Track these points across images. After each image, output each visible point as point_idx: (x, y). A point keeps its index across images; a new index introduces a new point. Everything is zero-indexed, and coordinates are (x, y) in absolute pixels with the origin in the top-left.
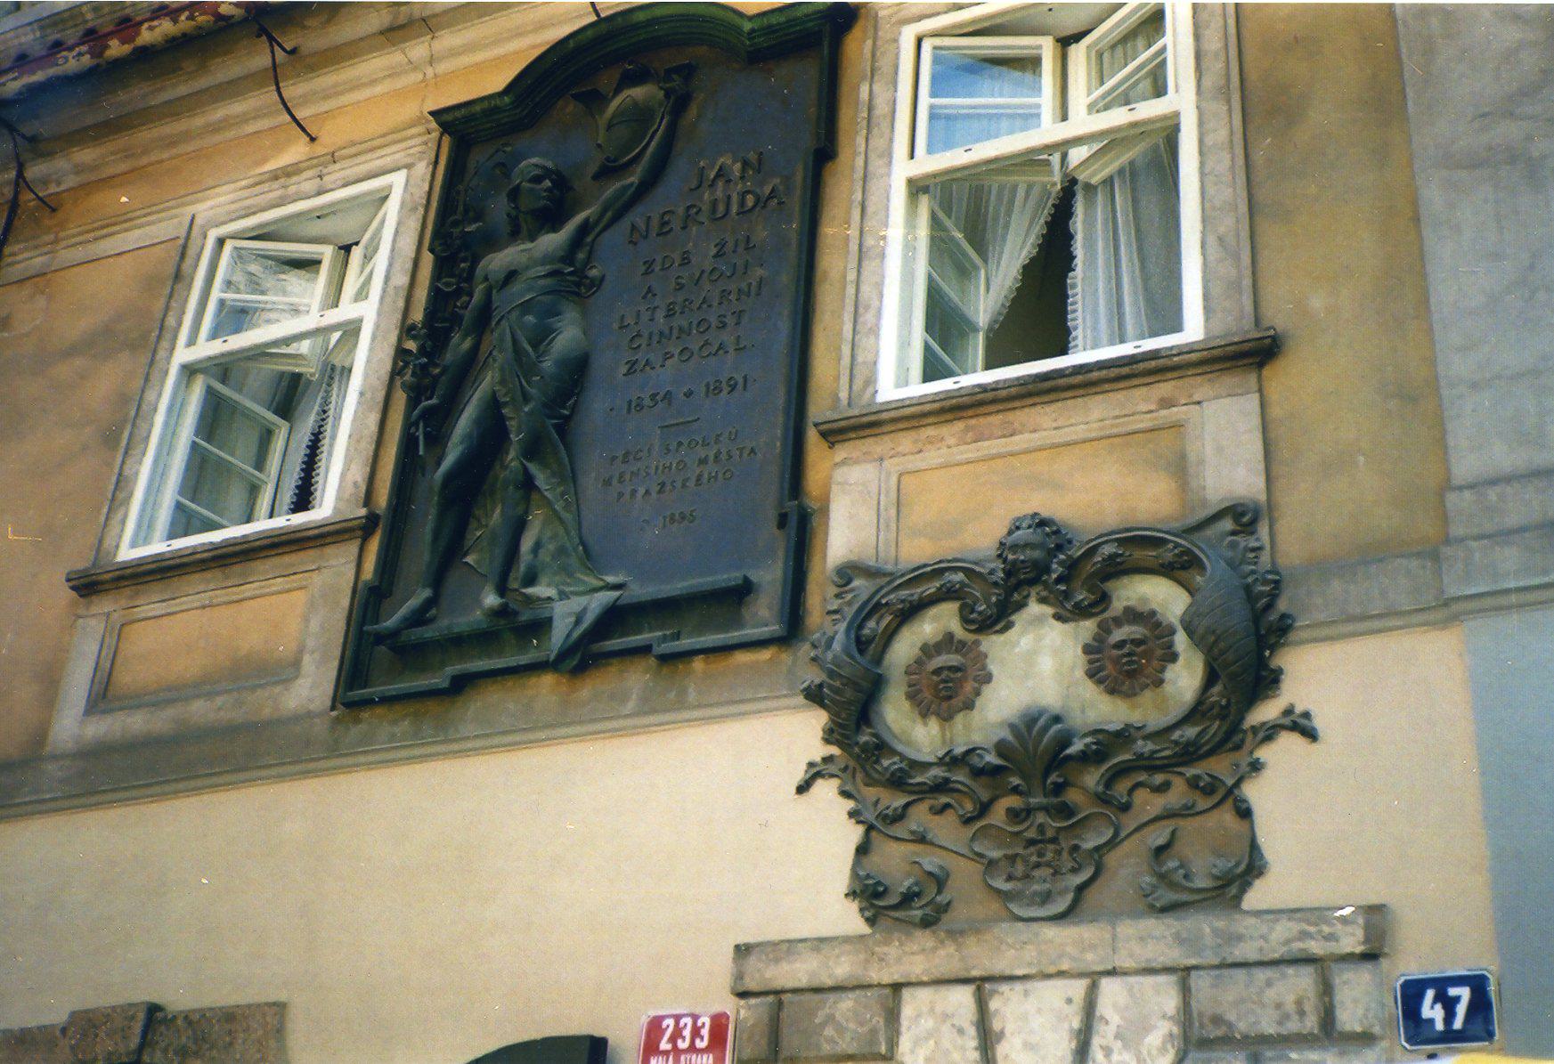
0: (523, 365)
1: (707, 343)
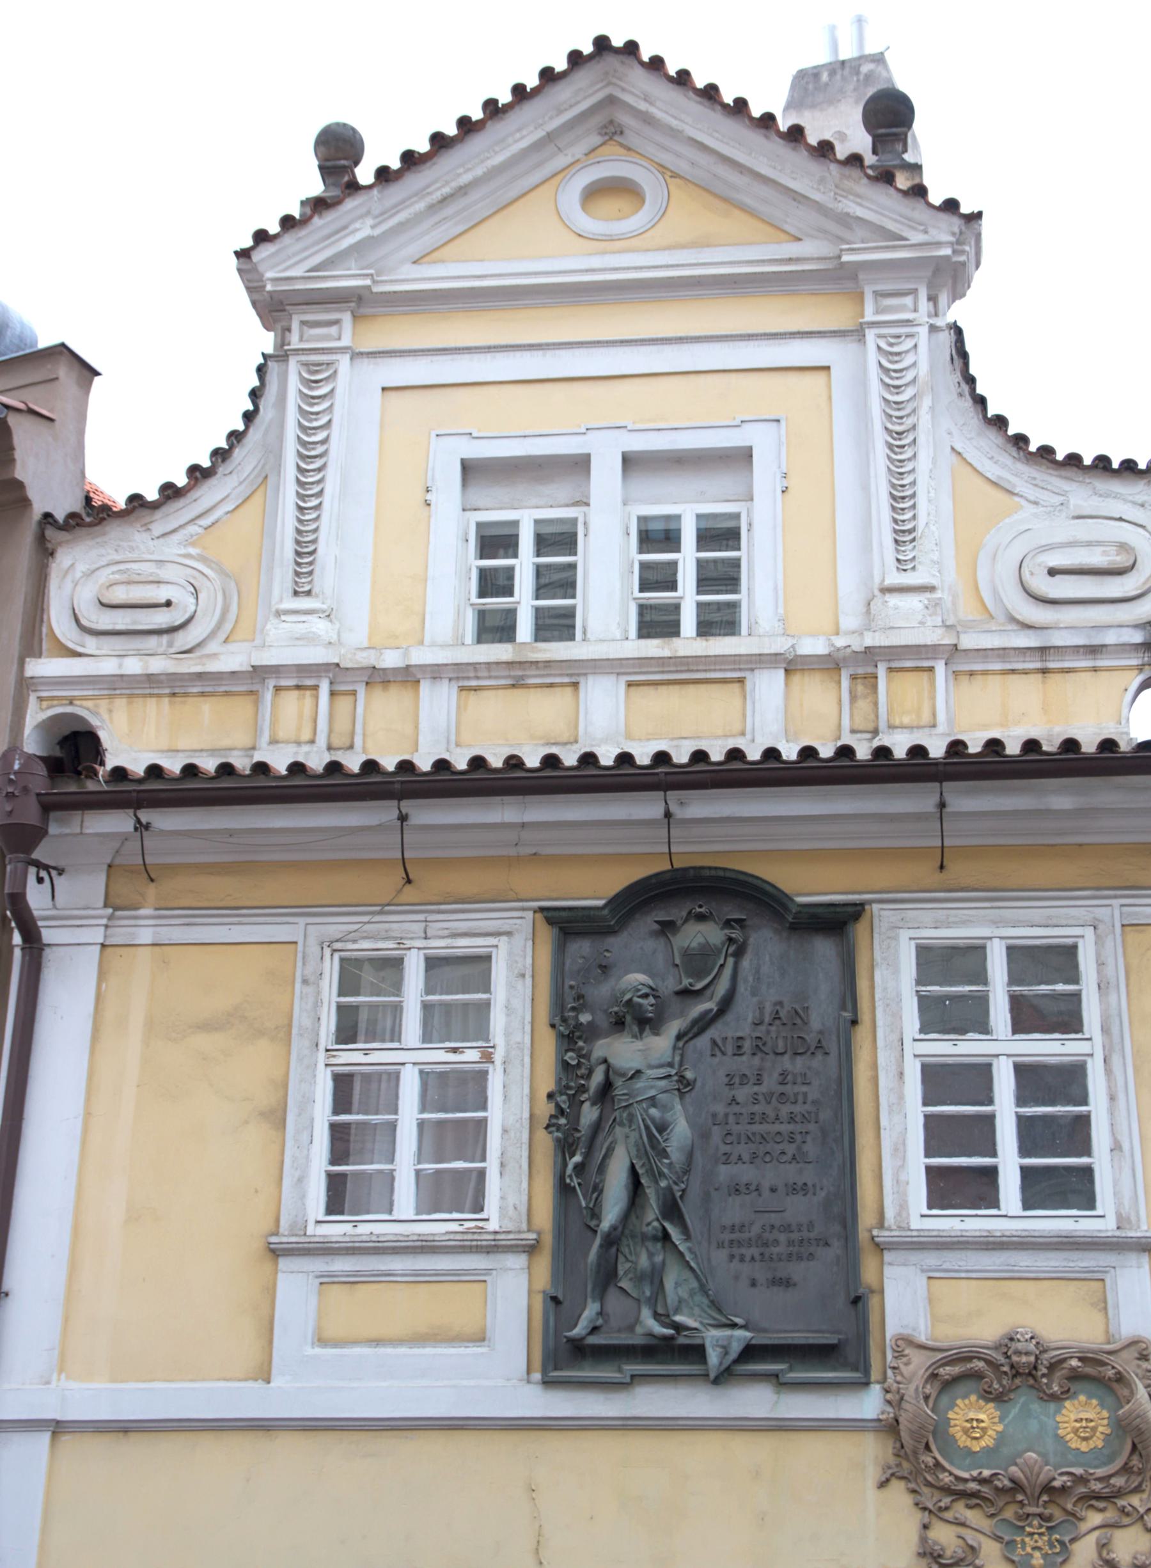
1: (783, 1153)
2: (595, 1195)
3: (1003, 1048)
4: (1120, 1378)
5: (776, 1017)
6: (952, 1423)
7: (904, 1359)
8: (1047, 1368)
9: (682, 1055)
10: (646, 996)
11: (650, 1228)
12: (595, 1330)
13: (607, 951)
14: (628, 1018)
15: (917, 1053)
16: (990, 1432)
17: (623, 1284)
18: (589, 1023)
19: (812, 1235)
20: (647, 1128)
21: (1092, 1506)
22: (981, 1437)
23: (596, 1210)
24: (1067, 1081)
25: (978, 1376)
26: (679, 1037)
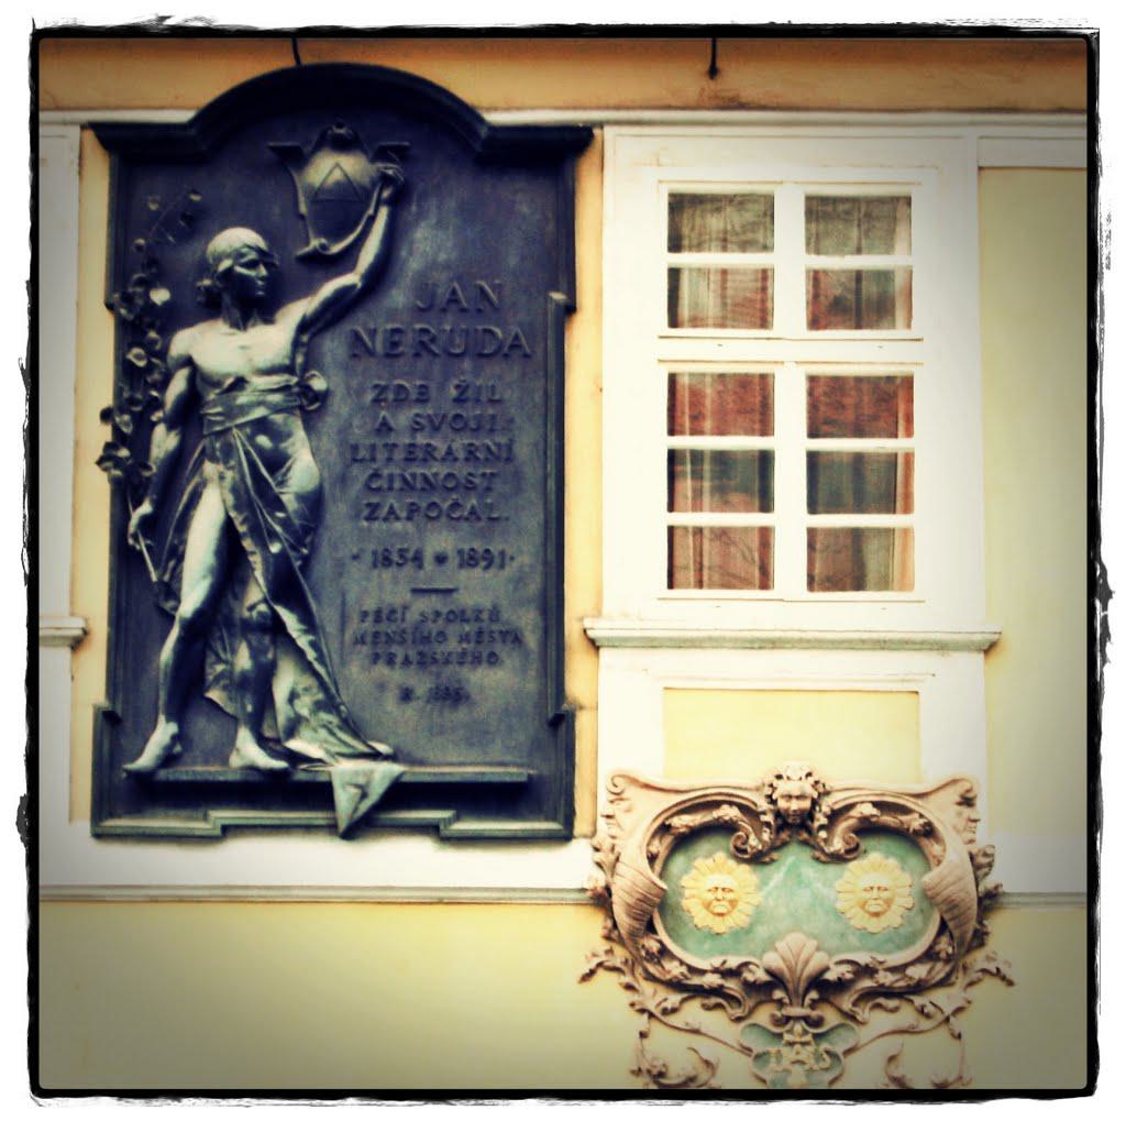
0: (257, 496)
2: (172, 564)
3: (793, 354)
4: (929, 831)
5: (453, 299)
6: (687, 893)
7: (623, 805)
8: (828, 817)
9: (307, 356)
10: (252, 265)
11: (254, 614)
12: (168, 759)
13: (196, 193)
14: (227, 299)
15: (661, 358)
16: (741, 906)
17: (215, 695)
18: (166, 304)
19: (495, 627)
20: (252, 465)
21: (879, 1006)
22: (729, 912)
23: (175, 586)
24: (882, 402)
25: (728, 828)
26: (304, 326)
